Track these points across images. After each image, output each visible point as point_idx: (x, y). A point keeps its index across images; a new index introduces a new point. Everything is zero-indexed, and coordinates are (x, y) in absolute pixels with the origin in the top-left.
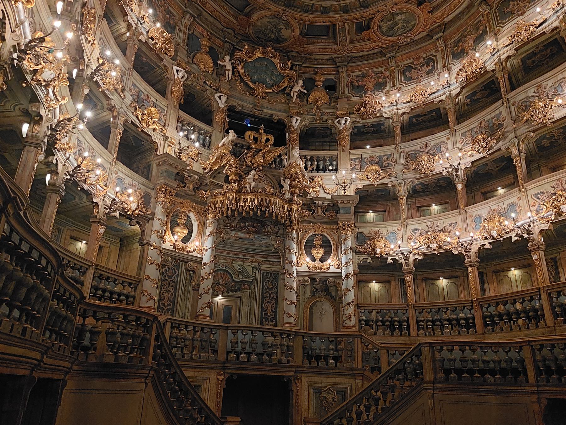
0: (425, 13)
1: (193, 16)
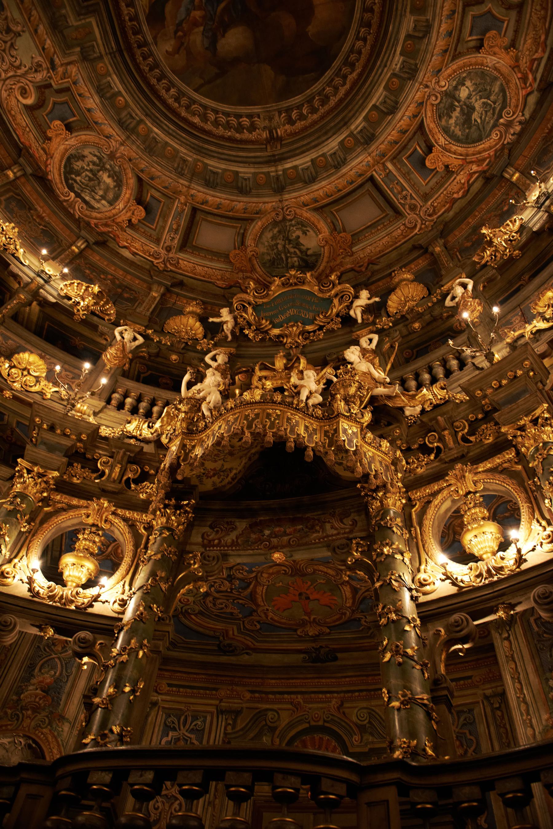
0: (503, 55)
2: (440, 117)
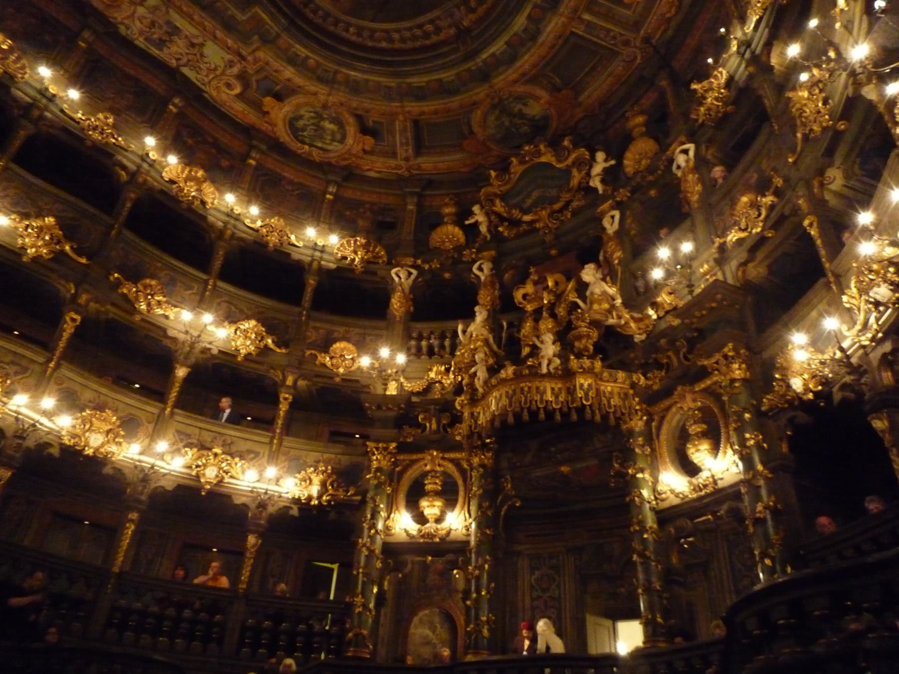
1: (416, 193)
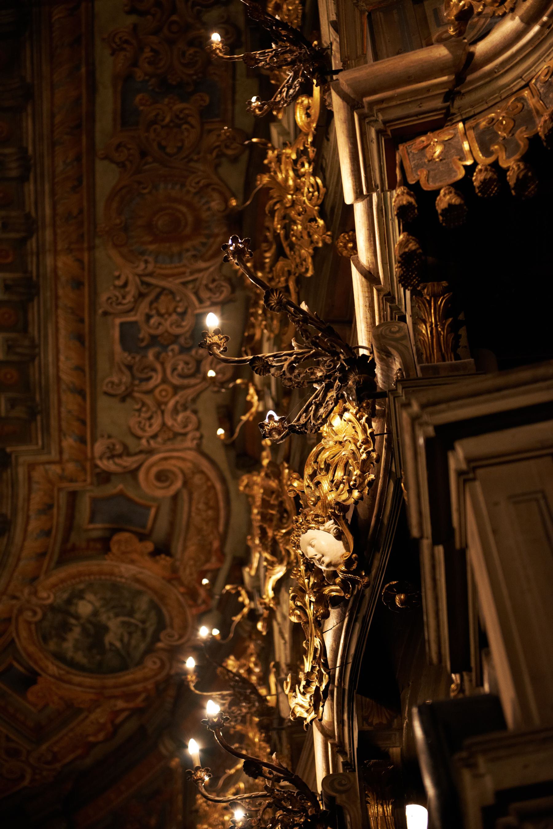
0: (148, 562)
2: (45, 639)
